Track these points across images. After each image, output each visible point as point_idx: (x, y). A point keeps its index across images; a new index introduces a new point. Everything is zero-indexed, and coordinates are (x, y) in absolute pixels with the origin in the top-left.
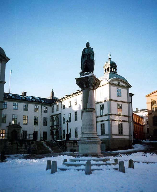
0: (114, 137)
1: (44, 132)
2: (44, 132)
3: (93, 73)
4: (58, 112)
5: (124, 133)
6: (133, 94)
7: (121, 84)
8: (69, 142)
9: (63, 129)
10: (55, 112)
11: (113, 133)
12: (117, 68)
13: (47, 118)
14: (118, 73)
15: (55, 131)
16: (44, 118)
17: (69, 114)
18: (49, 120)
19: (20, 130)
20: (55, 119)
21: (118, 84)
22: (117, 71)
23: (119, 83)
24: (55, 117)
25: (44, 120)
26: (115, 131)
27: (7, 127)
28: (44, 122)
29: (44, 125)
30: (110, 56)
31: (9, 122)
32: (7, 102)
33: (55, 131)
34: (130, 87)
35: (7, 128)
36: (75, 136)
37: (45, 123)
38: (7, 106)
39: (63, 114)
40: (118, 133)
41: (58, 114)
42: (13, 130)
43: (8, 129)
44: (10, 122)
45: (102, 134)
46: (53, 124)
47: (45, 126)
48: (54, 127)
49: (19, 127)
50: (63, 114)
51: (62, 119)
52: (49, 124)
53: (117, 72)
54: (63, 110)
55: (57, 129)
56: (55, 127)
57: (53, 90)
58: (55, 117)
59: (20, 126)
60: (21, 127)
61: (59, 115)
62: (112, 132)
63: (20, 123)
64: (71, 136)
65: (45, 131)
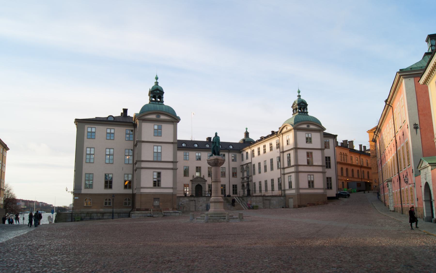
0: (301, 191)
1: (233, 185)
2: (233, 185)
4: (248, 160)
5: (316, 186)
6: (337, 135)
7: (312, 127)
8: (250, 197)
9: (254, 182)
10: (246, 161)
11: (301, 187)
13: (236, 168)
14: (309, 114)
15: (245, 184)
16: (233, 168)
17: (277, 157)
18: (239, 171)
19: (205, 184)
20: (245, 170)
21: (307, 128)
22: (308, 111)
23: (308, 126)
25: (232, 170)
26: (304, 184)
27: (191, 181)
28: (233, 174)
29: (233, 176)
30: (299, 92)
31: (192, 176)
32: (189, 152)
33: (245, 184)
34: (324, 129)
35: (191, 182)
36: (260, 191)
37: (234, 174)
38: (189, 156)
39: (253, 163)
40: (307, 187)
41: (247, 164)
42: (198, 184)
43: (192, 183)
44: (193, 175)
45: (289, 188)
46: (243, 175)
47: (234, 178)
49: (203, 180)
50: (253, 163)
51: (251, 169)
52: (240, 175)
54: (253, 159)
56: (245, 179)
57: (247, 129)
58: (245, 167)
59: (204, 179)
60: (206, 181)
61: (249, 165)
62: (299, 186)
63: (205, 176)
64: (256, 191)
65: (235, 184)
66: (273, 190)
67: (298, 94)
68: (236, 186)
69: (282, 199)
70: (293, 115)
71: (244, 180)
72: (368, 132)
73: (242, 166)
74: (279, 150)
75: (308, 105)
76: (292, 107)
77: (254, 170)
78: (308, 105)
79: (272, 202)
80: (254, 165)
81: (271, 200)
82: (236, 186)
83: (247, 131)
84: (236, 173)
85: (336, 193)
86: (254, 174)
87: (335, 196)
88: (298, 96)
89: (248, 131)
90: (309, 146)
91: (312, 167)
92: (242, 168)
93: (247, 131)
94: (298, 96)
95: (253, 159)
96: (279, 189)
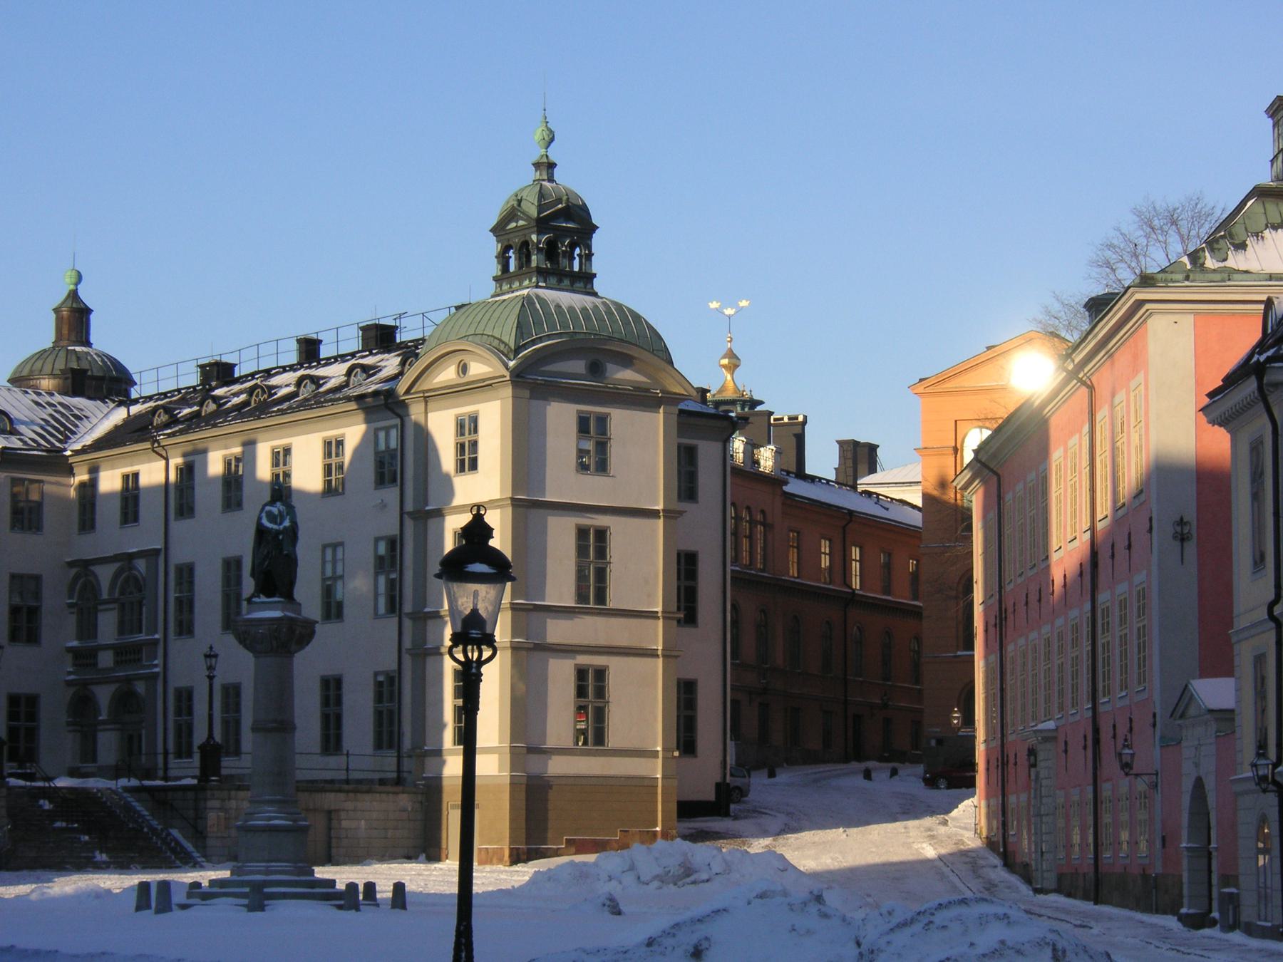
3: (289, 596)
4: (131, 530)
12: (597, 241)
13: (37, 579)
15: (104, 695)
20: (105, 596)
22: (597, 266)
23: (596, 369)
24: (105, 574)
33: (104, 695)
46: (87, 627)
48: (95, 656)
50: (179, 555)
51: (166, 593)
53: (594, 271)
54: (180, 528)
55: (129, 680)
56: (106, 659)
58: (105, 574)
66: (332, 740)
67: (537, 153)
68: (33, 701)
69: (404, 810)
70: (496, 279)
71: (95, 664)
72: (921, 390)
73: (85, 565)
74: (392, 494)
75: (595, 228)
76: (499, 230)
77: (186, 605)
78: (595, 228)
79: (345, 824)
80: (186, 574)
81: (343, 815)
82: (33, 701)
83: (74, 295)
84: (34, 612)
85: (719, 780)
86: (186, 628)
87: (710, 795)
88: (537, 165)
89: (86, 296)
90: (591, 490)
91: (600, 622)
92: (76, 578)
93: (74, 295)
94: (537, 165)
95: (177, 527)
96: (379, 745)
